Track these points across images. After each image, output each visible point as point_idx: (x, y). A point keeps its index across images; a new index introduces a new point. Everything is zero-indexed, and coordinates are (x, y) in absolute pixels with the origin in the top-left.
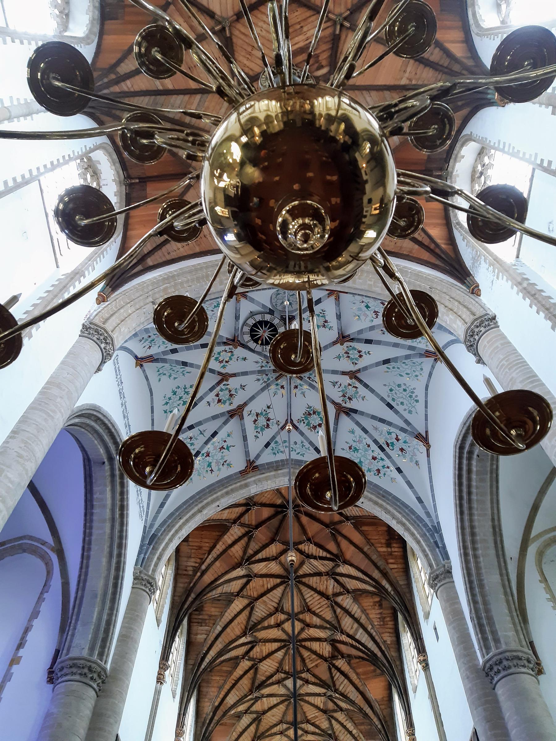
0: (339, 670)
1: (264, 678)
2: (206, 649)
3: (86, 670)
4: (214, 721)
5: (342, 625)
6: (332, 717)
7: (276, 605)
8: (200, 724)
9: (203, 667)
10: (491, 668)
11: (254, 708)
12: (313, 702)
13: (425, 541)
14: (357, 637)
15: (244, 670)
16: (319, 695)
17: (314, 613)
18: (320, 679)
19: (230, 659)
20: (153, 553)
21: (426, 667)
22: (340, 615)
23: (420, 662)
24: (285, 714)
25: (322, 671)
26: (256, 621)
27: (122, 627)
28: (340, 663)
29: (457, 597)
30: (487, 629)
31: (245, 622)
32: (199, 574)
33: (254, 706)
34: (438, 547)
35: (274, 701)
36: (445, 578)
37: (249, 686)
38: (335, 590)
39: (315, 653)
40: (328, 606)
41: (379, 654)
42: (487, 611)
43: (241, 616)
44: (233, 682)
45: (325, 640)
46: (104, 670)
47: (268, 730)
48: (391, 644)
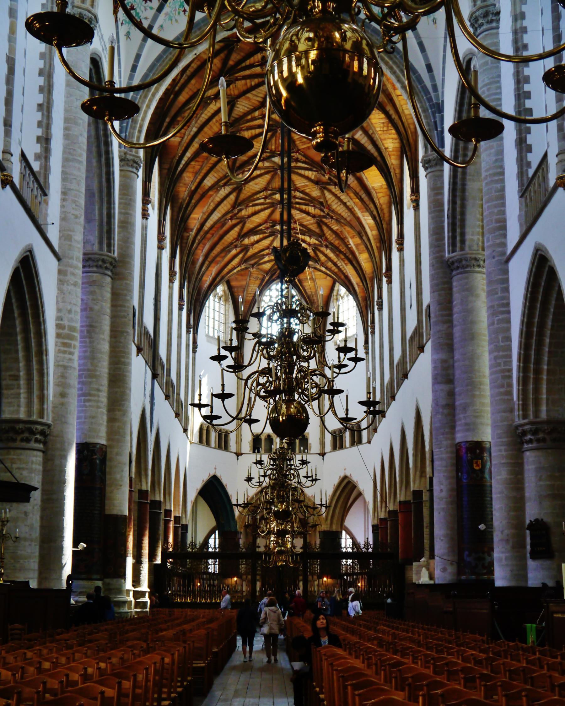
3: (100, 263)
4: (191, 205)
7: (260, 99)
9: (179, 169)
10: (453, 263)
13: (426, 117)
20: (134, 128)
21: (417, 207)
23: (412, 201)
26: (237, 117)
27: (120, 213)
29: (442, 188)
30: (458, 230)
32: (172, 96)
34: (437, 130)
36: (436, 164)
41: (379, 158)
42: (463, 214)
46: (114, 259)
48: (393, 151)
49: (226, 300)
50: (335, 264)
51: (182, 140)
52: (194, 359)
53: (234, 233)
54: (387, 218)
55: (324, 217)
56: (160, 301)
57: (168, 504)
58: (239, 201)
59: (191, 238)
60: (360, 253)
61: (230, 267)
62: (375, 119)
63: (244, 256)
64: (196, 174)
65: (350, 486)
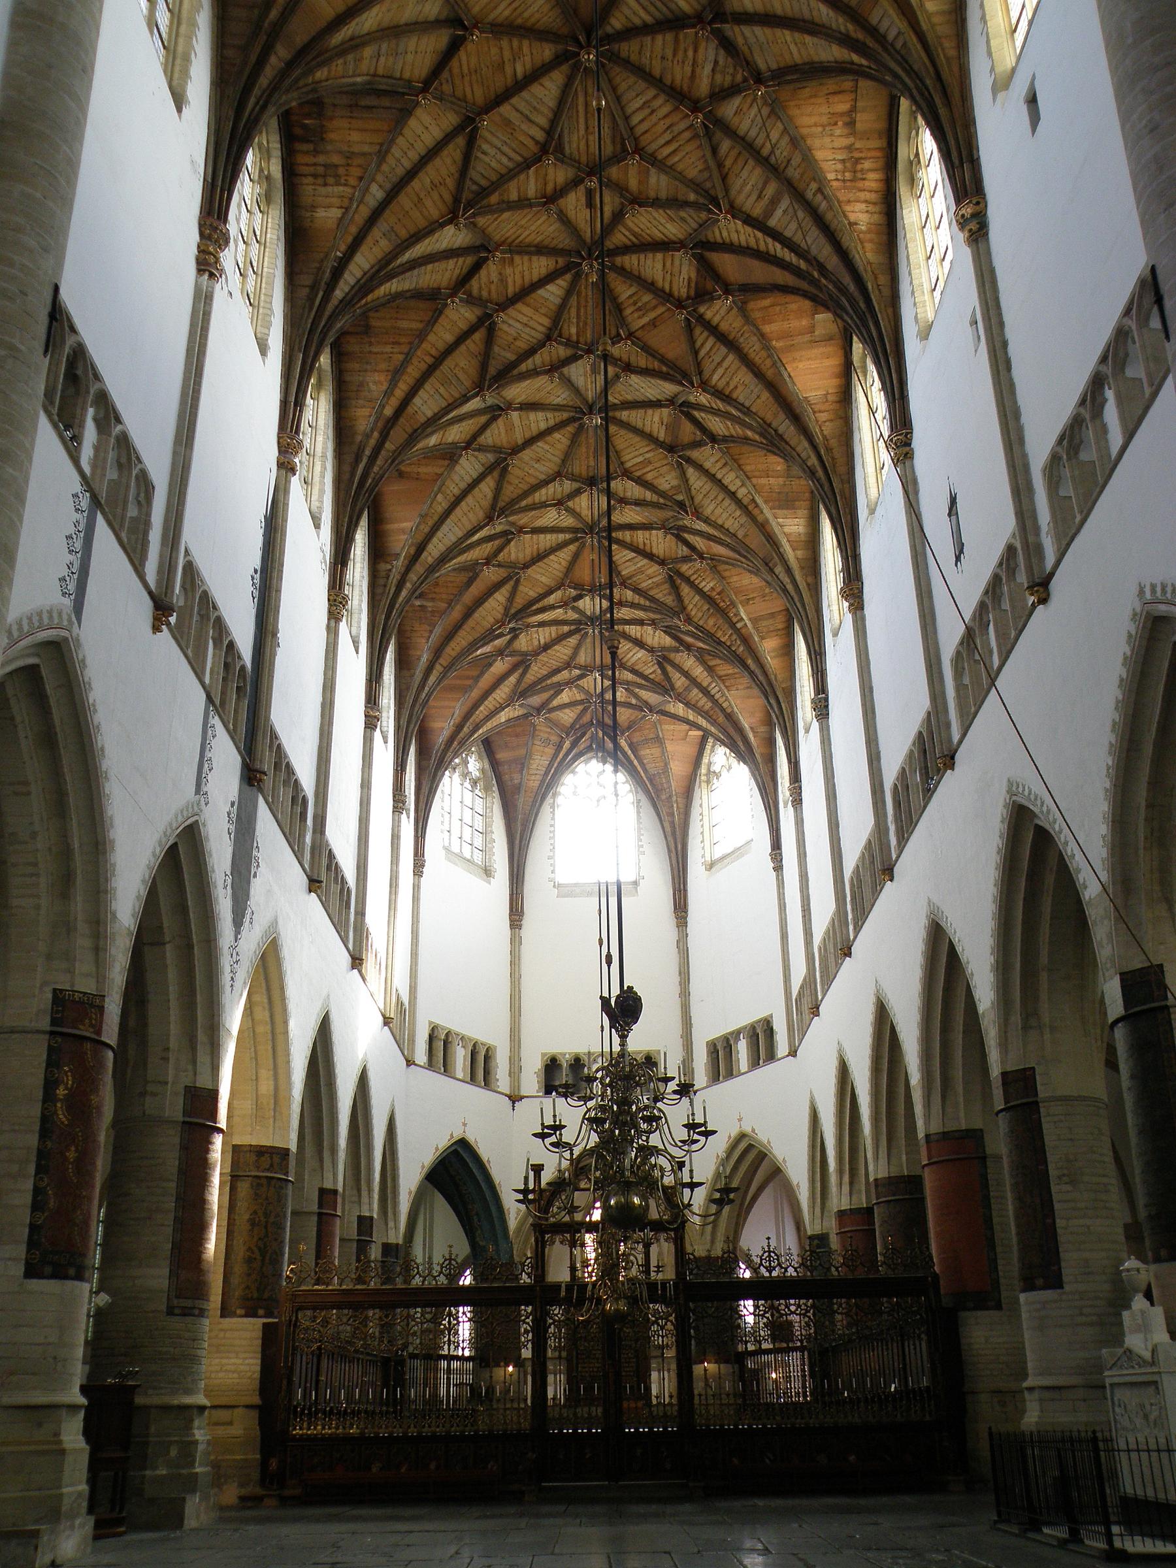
0: (713, 330)
1: (512, 357)
2: (343, 248)
5: (733, 193)
6: (689, 460)
8: (349, 458)
9: (338, 294)
11: (487, 438)
12: (639, 425)
14: (772, 222)
15: (457, 331)
16: (656, 404)
17: (653, 160)
18: (663, 360)
19: (419, 295)
22: (728, 163)
24: (567, 457)
25: (669, 339)
26: (484, 183)
28: (719, 311)
31: (451, 183)
33: (488, 433)
35: (539, 421)
37: (473, 372)
38: (718, 78)
39: (649, 286)
40: (696, 136)
43: (437, 161)
44: (430, 360)
45: (680, 245)
47: (526, 494)
48: (869, 231)
49: (487, 789)
50: (705, 691)
51: (344, 214)
52: (416, 888)
53: (495, 605)
54: (842, 469)
55: (686, 559)
56: (279, 591)
57: (328, 1175)
58: (501, 504)
59: (395, 577)
60: (762, 638)
61: (490, 703)
62: (822, 148)
63: (519, 681)
64: (397, 374)
65: (751, 1157)
